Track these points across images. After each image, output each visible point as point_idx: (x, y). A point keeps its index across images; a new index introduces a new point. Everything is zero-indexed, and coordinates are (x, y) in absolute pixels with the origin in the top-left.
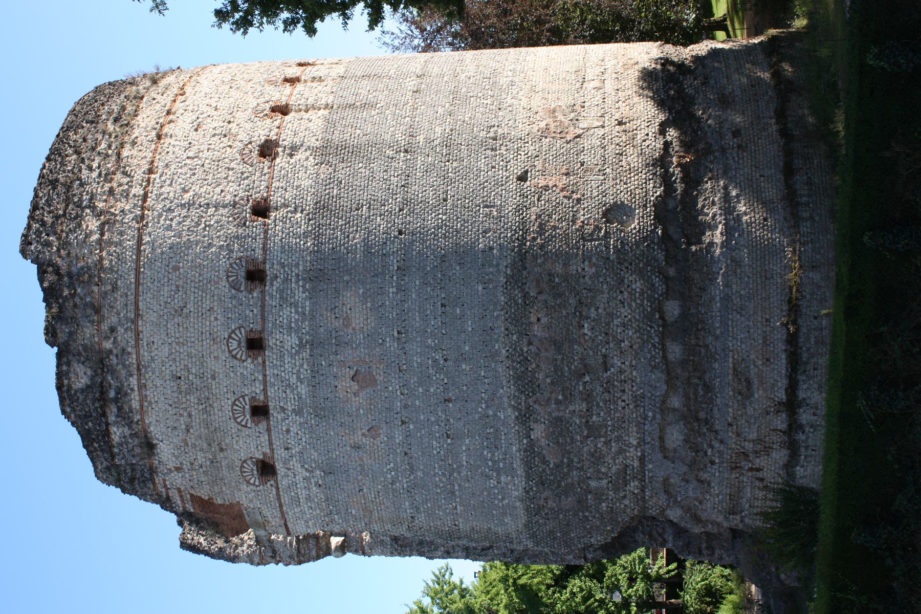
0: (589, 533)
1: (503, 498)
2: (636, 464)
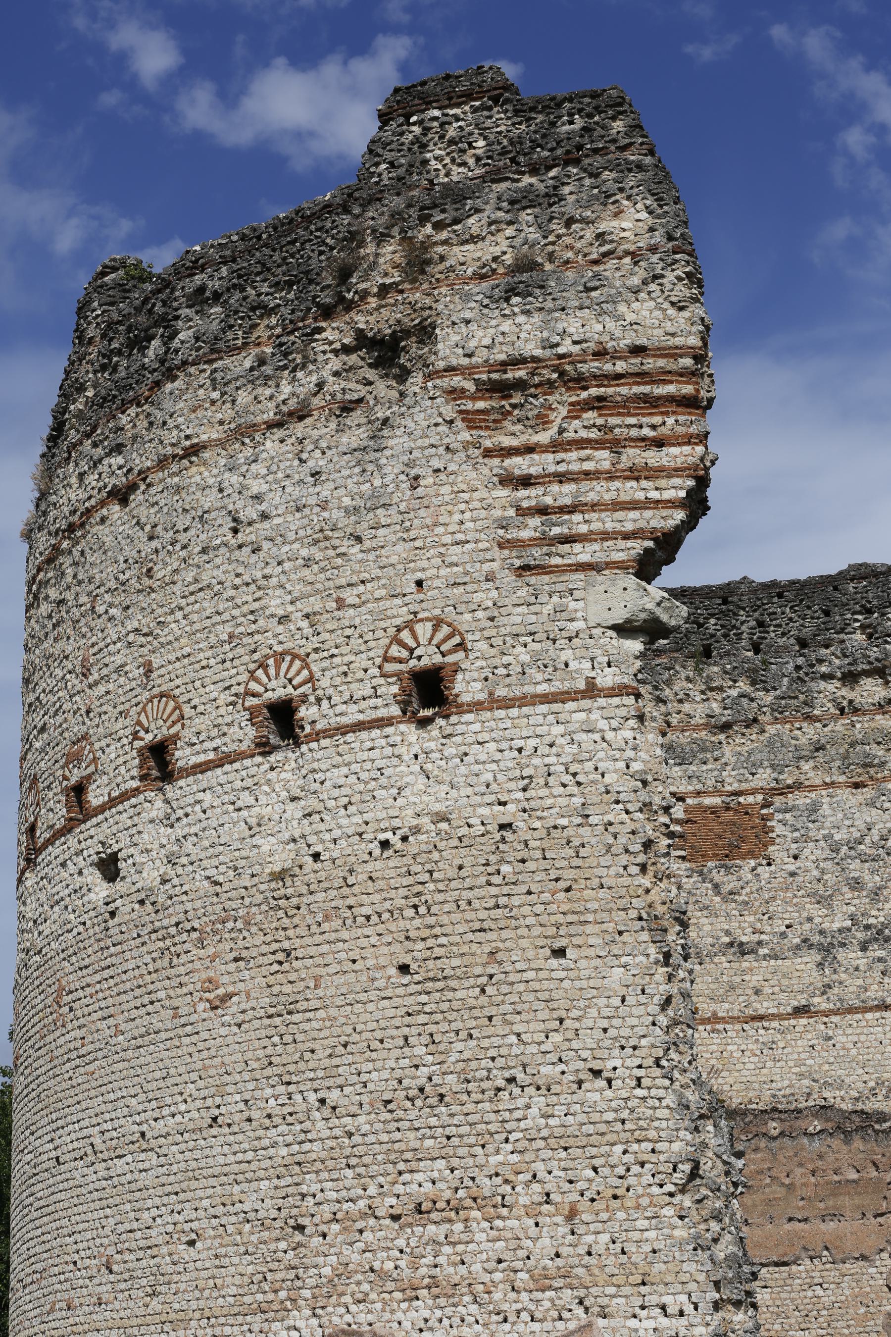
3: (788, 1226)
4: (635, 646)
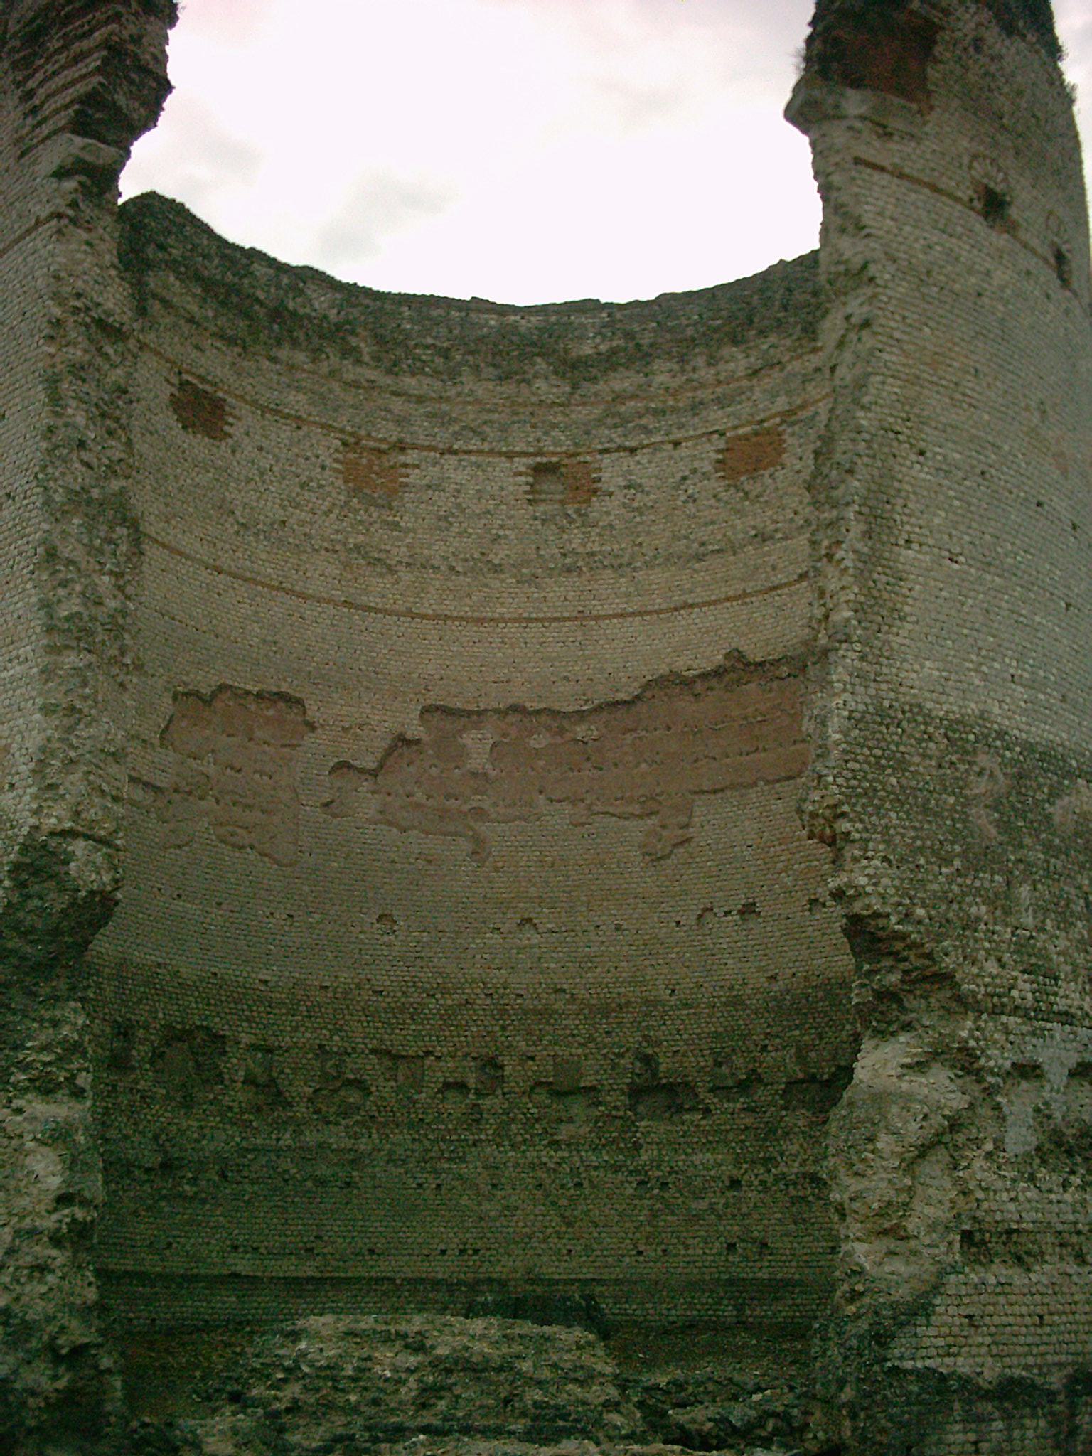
0: (902, 860)
1: (985, 678)
2: (1061, 1005)
3: (793, 748)
4: (70, 185)
